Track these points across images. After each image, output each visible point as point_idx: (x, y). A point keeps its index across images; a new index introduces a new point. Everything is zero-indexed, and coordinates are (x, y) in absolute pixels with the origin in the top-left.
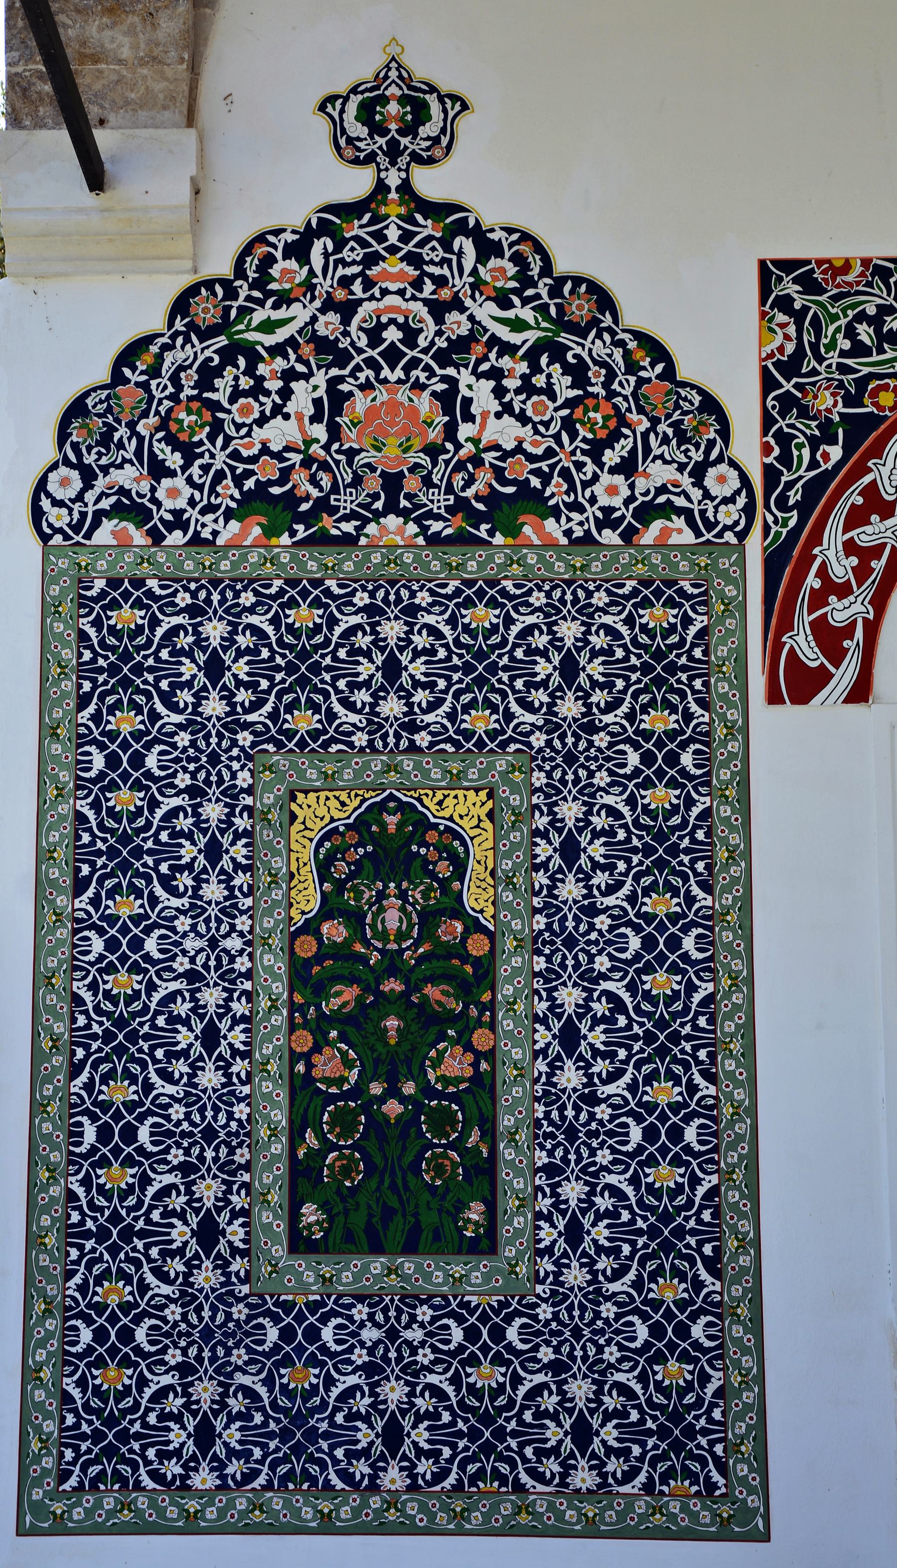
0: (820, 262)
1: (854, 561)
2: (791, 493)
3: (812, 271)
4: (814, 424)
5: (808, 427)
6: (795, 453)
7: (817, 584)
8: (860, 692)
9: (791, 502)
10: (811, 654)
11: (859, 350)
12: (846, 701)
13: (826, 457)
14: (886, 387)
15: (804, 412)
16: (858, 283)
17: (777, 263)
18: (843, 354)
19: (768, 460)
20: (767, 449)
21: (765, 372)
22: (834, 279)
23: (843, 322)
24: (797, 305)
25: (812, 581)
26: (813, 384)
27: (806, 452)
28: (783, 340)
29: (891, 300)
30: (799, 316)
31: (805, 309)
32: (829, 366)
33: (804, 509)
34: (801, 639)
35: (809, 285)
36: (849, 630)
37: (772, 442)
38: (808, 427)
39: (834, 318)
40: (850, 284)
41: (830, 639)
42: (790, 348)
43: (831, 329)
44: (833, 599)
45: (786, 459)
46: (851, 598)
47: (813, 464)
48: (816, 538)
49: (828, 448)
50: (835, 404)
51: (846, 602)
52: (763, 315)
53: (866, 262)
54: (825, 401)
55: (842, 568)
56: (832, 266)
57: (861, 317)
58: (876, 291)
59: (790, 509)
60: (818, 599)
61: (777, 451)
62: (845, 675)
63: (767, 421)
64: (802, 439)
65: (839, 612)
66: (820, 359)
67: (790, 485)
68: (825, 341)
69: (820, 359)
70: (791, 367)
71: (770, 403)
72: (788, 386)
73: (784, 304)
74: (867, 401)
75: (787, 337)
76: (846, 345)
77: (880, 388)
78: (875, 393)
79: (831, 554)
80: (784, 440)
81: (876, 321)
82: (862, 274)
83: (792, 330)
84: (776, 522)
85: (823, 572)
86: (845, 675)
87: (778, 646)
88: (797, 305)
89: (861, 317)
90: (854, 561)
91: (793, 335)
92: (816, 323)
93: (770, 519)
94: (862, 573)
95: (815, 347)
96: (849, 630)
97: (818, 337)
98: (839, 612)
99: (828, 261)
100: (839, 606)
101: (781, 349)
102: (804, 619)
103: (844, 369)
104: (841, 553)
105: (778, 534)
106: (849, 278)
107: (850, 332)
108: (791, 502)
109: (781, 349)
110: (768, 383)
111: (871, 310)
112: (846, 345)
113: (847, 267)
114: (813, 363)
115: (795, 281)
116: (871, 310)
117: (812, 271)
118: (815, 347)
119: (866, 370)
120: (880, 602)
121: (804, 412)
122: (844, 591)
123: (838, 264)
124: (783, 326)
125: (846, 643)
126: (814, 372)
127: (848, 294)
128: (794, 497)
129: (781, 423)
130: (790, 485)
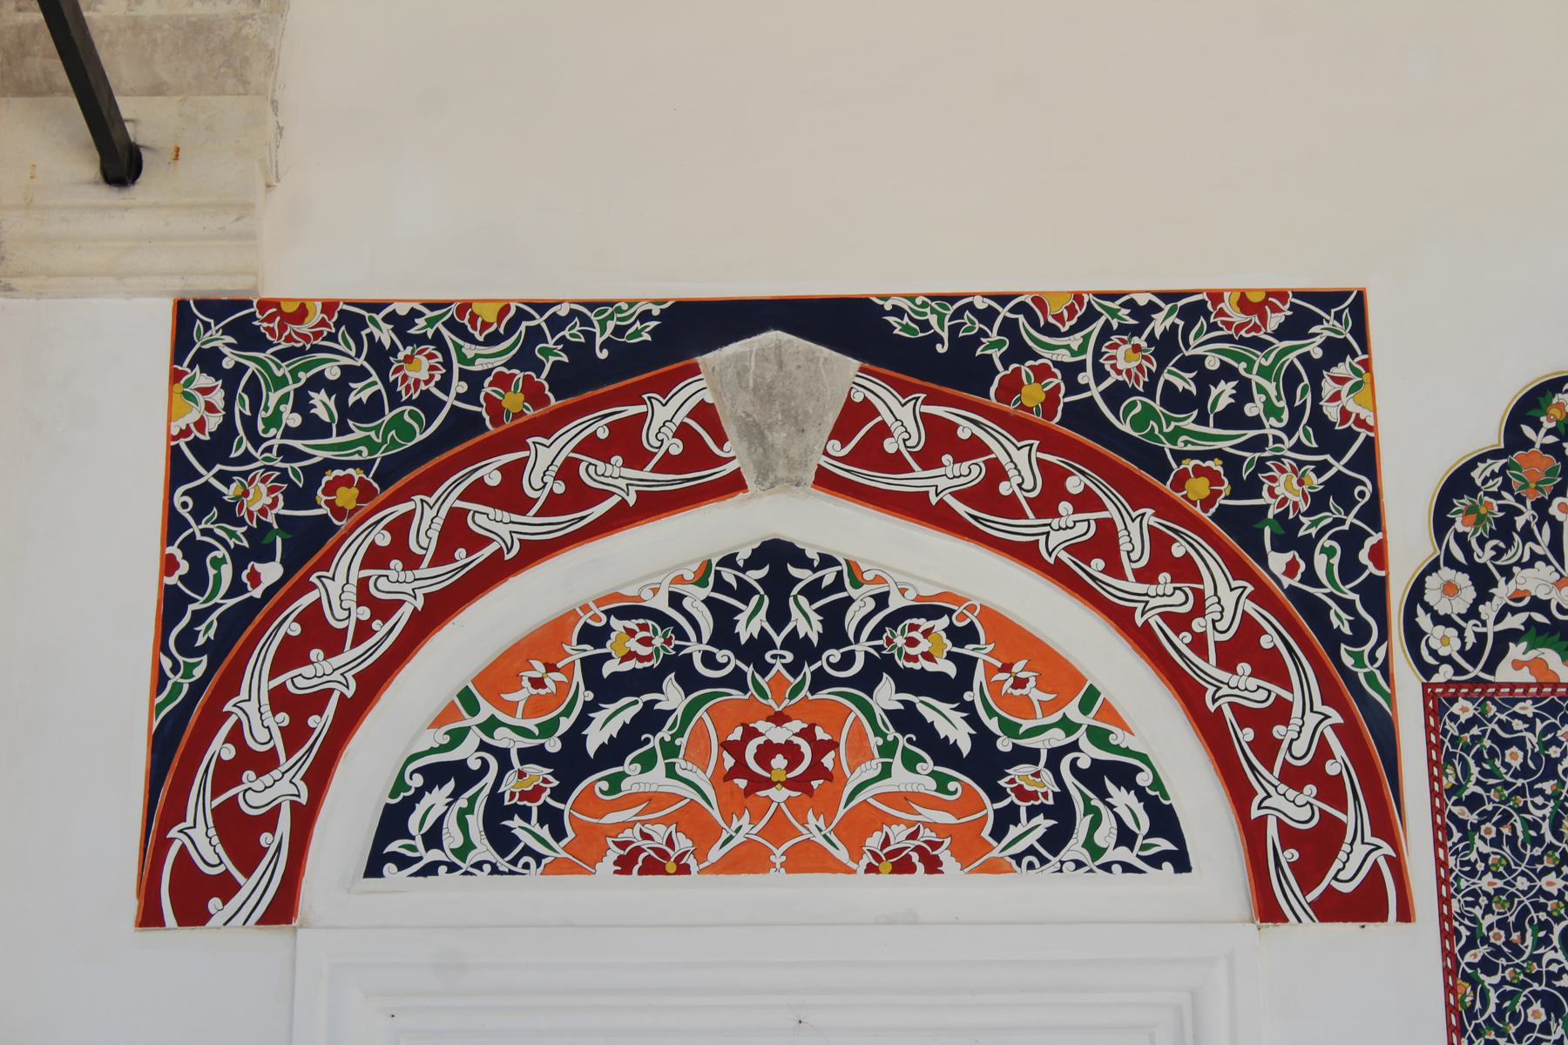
0: (264, 305)
1: (284, 718)
2: (202, 627)
3: (252, 316)
4: (240, 530)
5: (232, 534)
6: (212, 572)
7: (229, 753)
8: (282, 910)
9: (201, 641)
10: (210, 853)
11: (313, 428)
12: (265, 920)
13: (255, 578)
14: (347, 481)
15: (229, 514)
16: (317, 335)
17: (203, 305)
18: (289, 433)
19: (172, 580)
20: (169, 565)
21: (175, 455)
22: (282, 328)
23: (291, 388)
24: (228, 364)
25: (221, 748)
26: (245, 475)
27: (227, 571)
28: (204, 409)
29: (361, 362)
30: (230, 379)
31: (240, 369)
32: (269, 449)
33: (214, 651)
34: (198, 834)
35: (248, 337)
36: (269, 820)
37: (179, 554)
38: (232, 534)
39: (280, 382)
40: (305, 337)
41: (242, 835)
42: (214, 422)
43: (274, 397)
44: (249, 775)
45: (197, 579)
46: (276, 774)
47: (237, 588)
48: (231, 686)
49: (259, 567)
50: (274, 505)
51: (267, 779)
52: (176, 376)
53: (329, 307)
54: (260, 499)
55: (265, 729)
56: (280, 312)
57: (318, 382)
58: (342, 348)
59: (199, 652)
60: (227, 775)
61: (184, 567)
62: (258, 887)
63: (174, 524)
64: (221, 552)
65: (256, 794)
66: (256, 440)
67: (200, 616)
68: (262, 414)
69: (256, 440)
70: (215, 449)
71: (178, 499)
72: (208, 477)
73: (209, 361)
74: (321, 497)
75: (210, 408)
76: (295, 420)
77: (339, 482)
78: (331, 489)
79: (251, 707)
80: (195, 551)
81: (339, 389)
82: (323, 323)
83: (218, 398)
84: (175, 670)
85: (236, 736)
86: (258, 887)
87: (164, 843)
88: (228, 364)
89: (318, 382)
90: (284, 718)
91: (220, 404)
92: (254, 389)
93: (167, 664)
94: (295, 736)
95: (250, 423)
96: (269, 820)
97: (255, 407)
98: (256, 794)
99: (276, 303)
100: (258, 785)
101: (200, 425)
102: (200, 804)
103: (288, 454)
104: (266, 708)
105: (177, 687)
106: (304, 329)
107: (302, 403)
108: (201, 641)
109: (200, 425)
110: (178, 471)
111: (333, 373)
112: (295, 420)
113: (301, 314)
114: (246, 444)
115: (227, 330)
116: (333, 373)
117: (252, 316)
118: (250, 423)
119: (321, 455)
120: (318, 778)
121: (229, 514)
122: (265, 763)
123: (289, 308)
124: (206, 391)
125: (265, 839)
126: (247, 458)
127: (301, 352)
128: (206, 633)
129: (196, 529)
130: (200, 616)
